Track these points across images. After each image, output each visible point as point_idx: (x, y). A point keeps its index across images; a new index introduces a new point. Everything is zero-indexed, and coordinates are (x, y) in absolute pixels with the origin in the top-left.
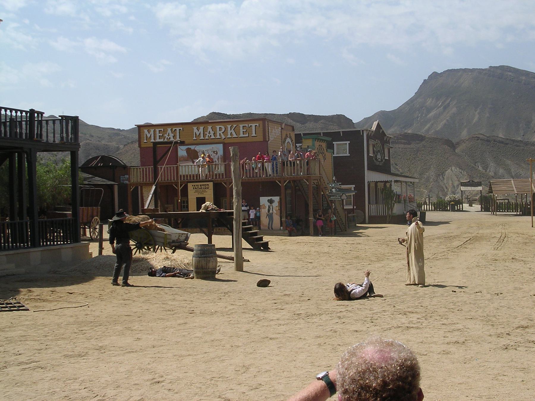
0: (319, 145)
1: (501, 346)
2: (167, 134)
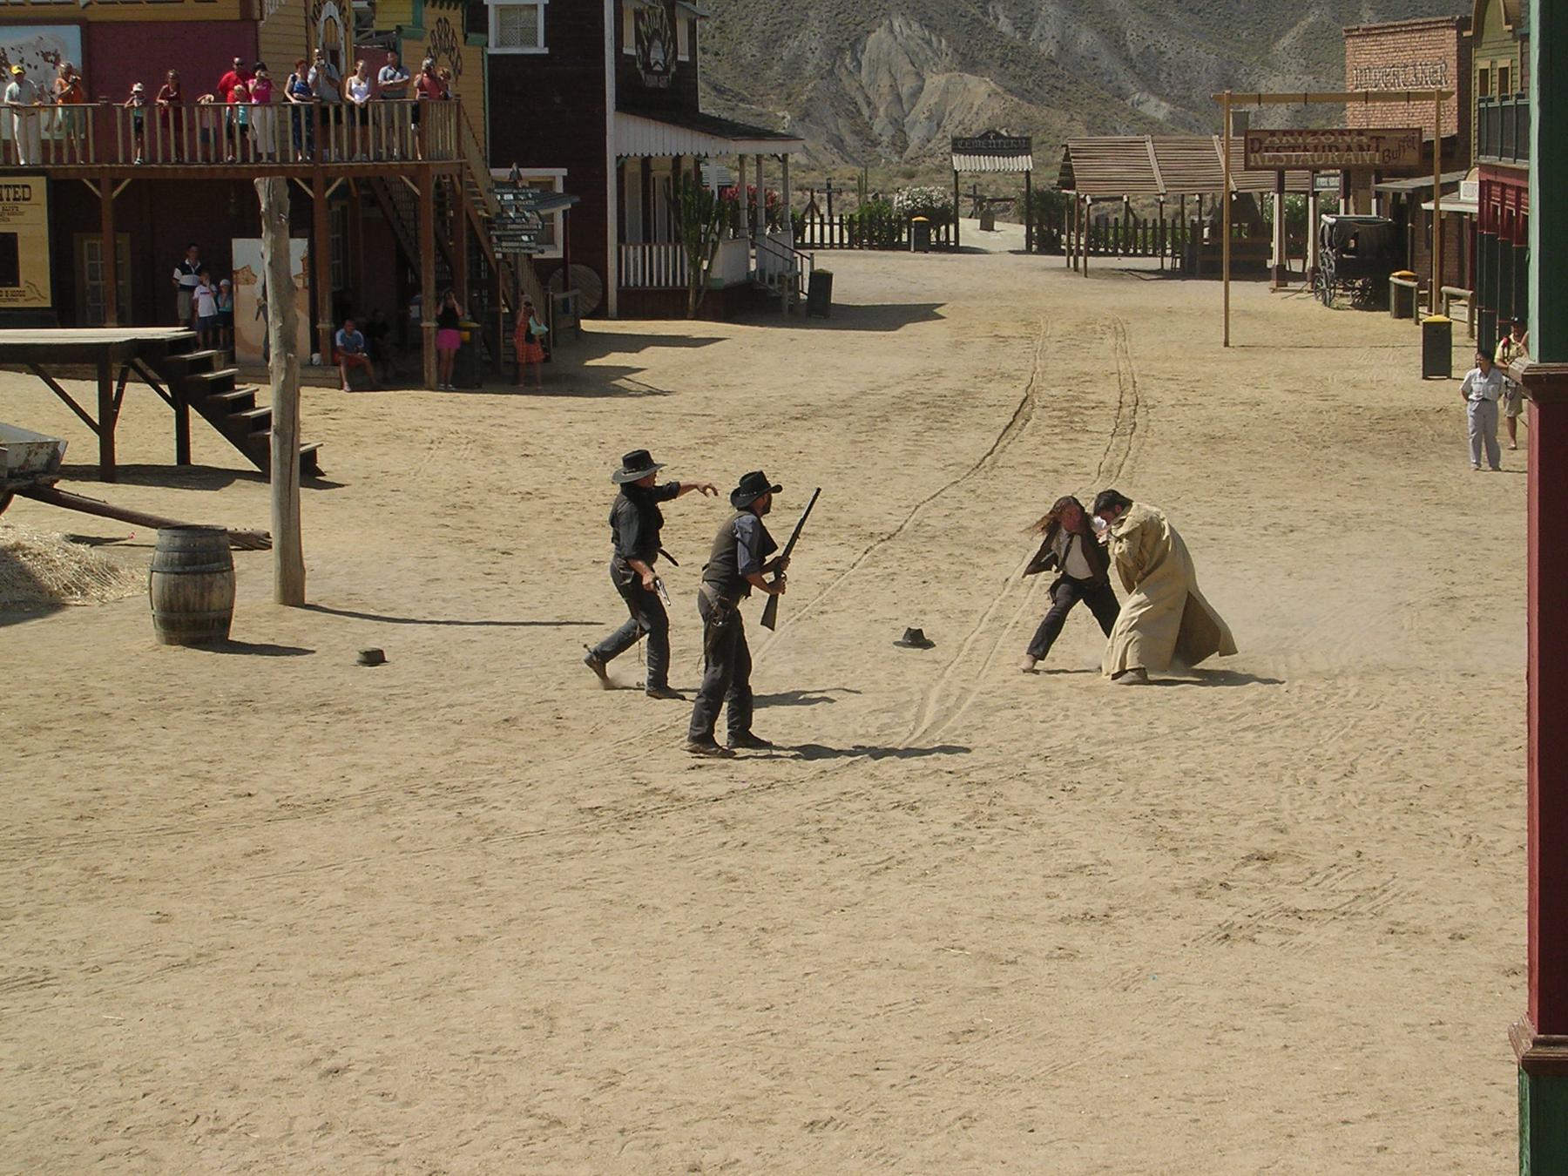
0: (440, 20)
1: (1211, 928)
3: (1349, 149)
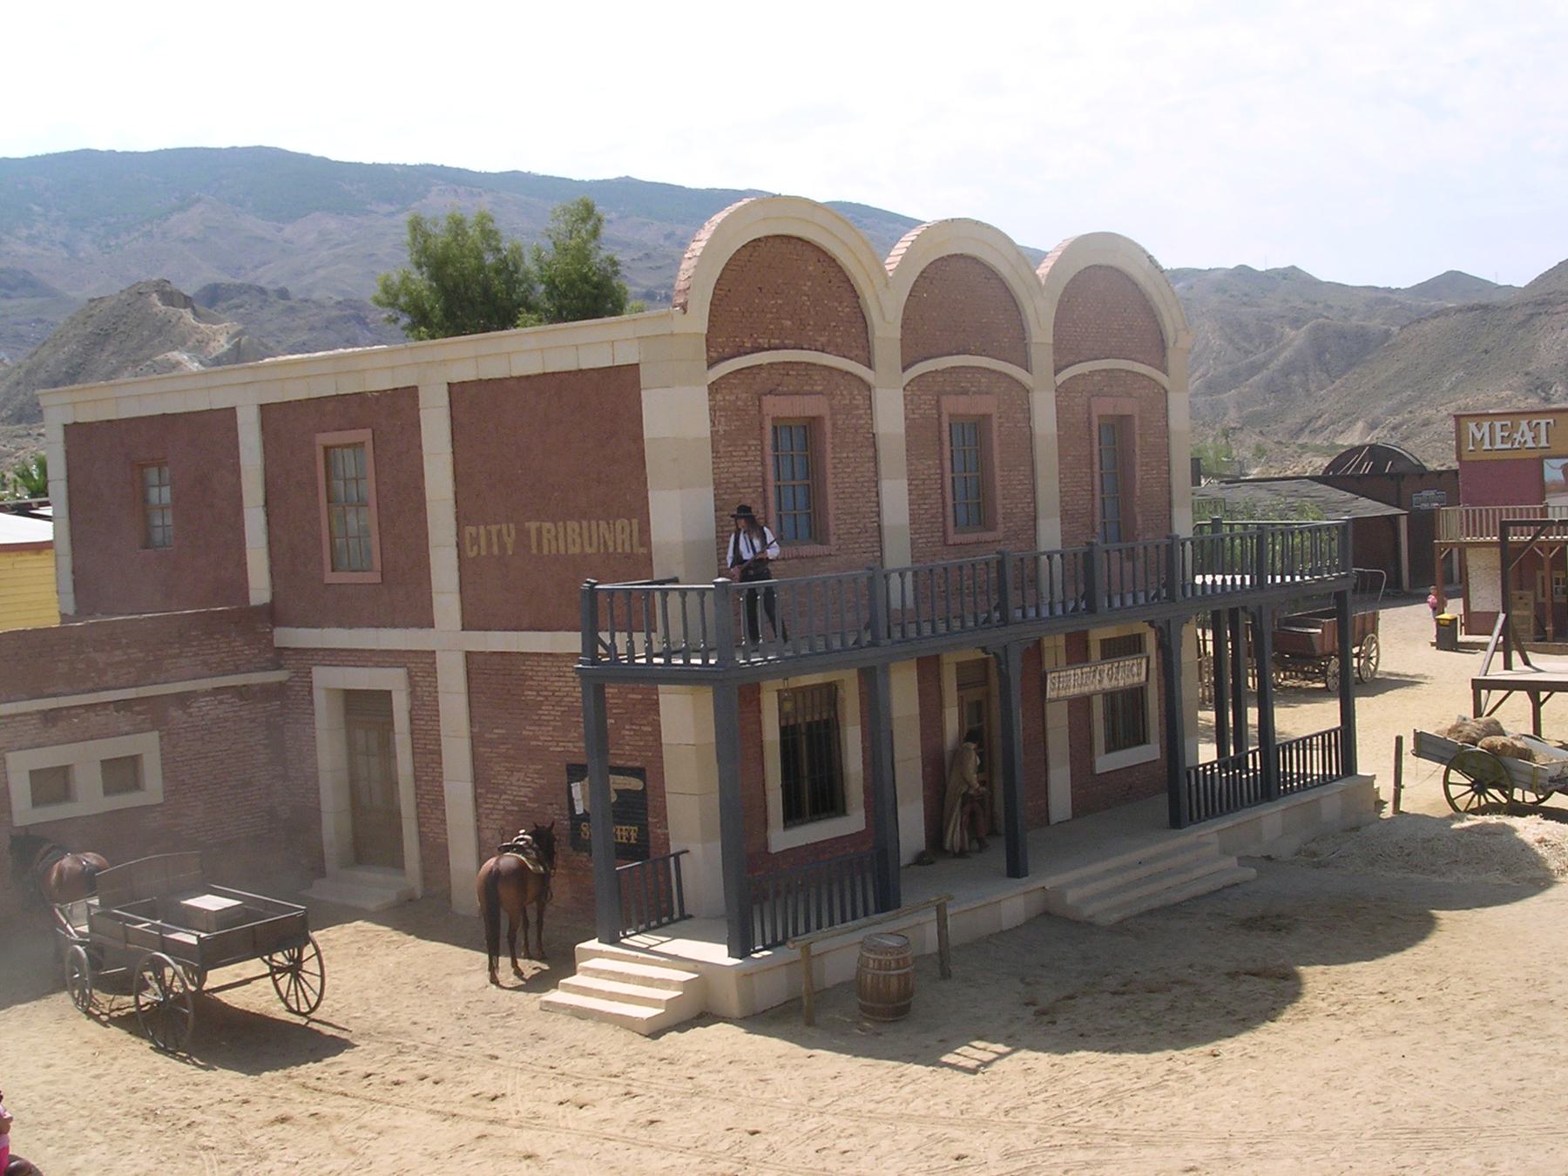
2: (1520, 433)
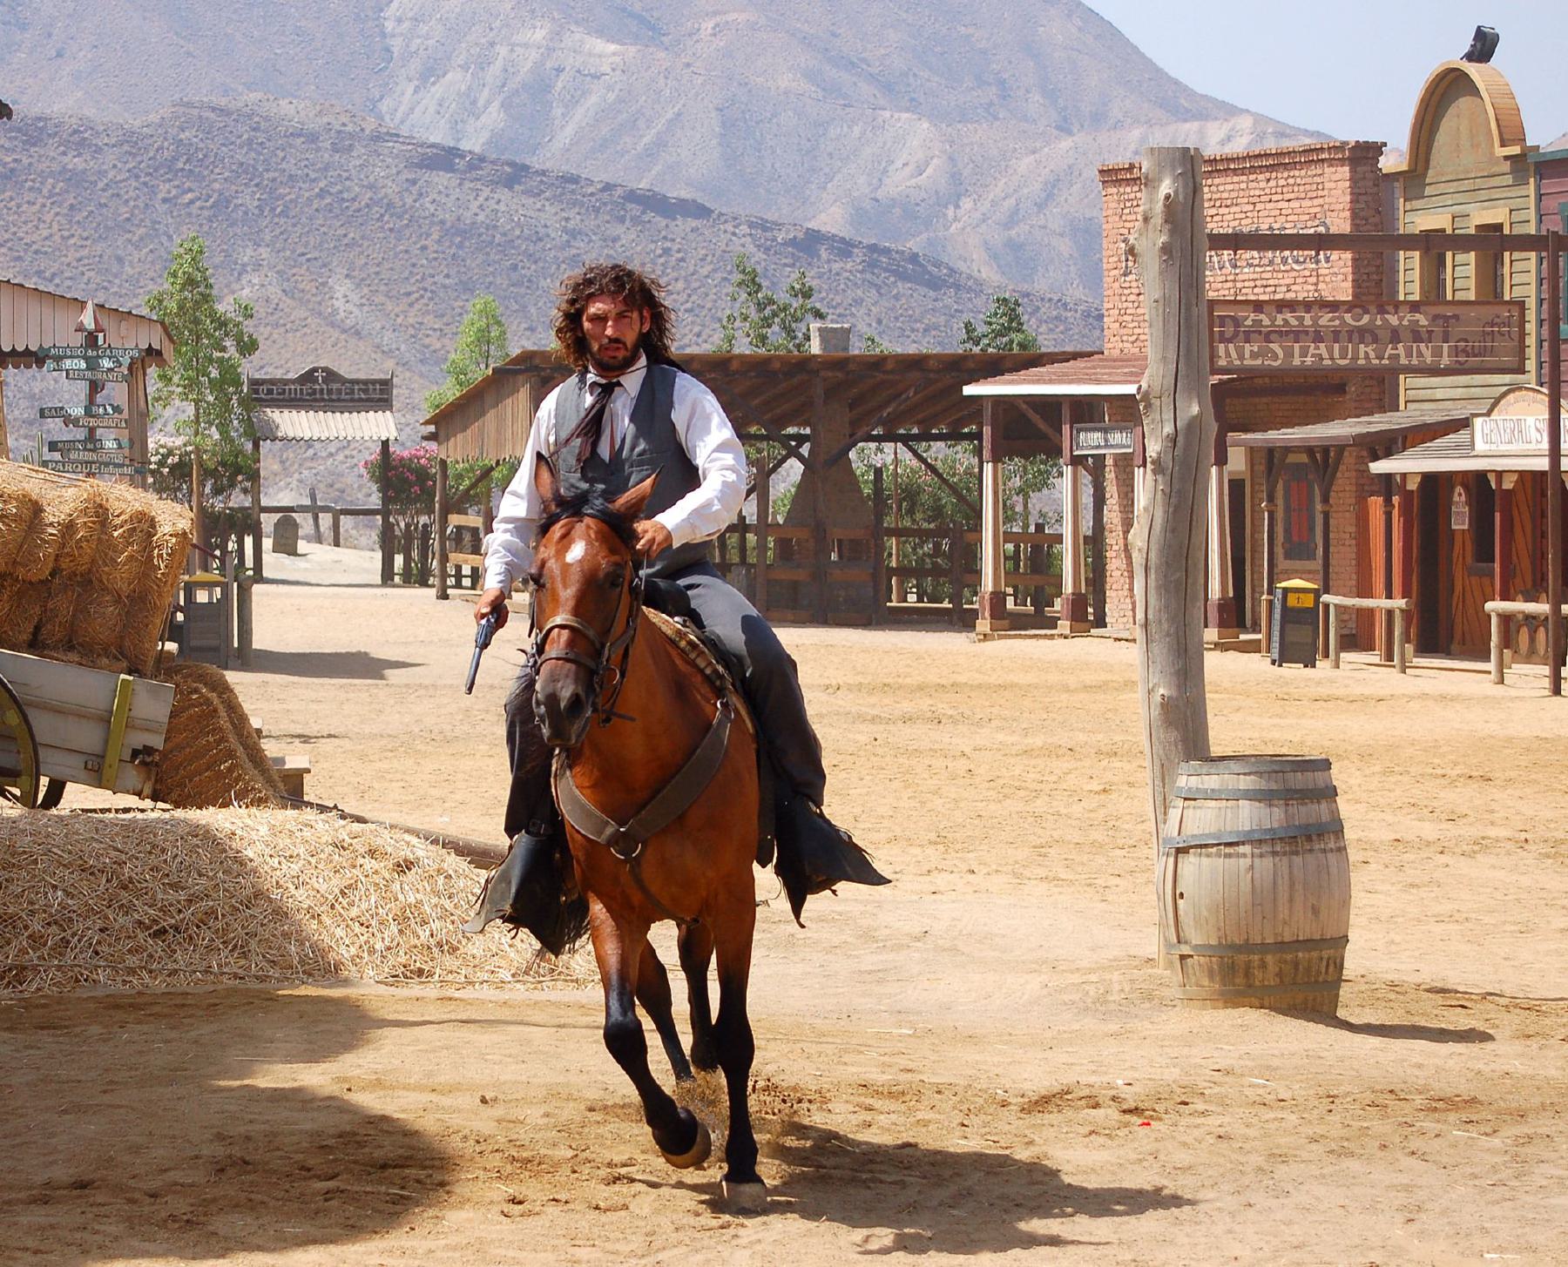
3: (1395, 337)
